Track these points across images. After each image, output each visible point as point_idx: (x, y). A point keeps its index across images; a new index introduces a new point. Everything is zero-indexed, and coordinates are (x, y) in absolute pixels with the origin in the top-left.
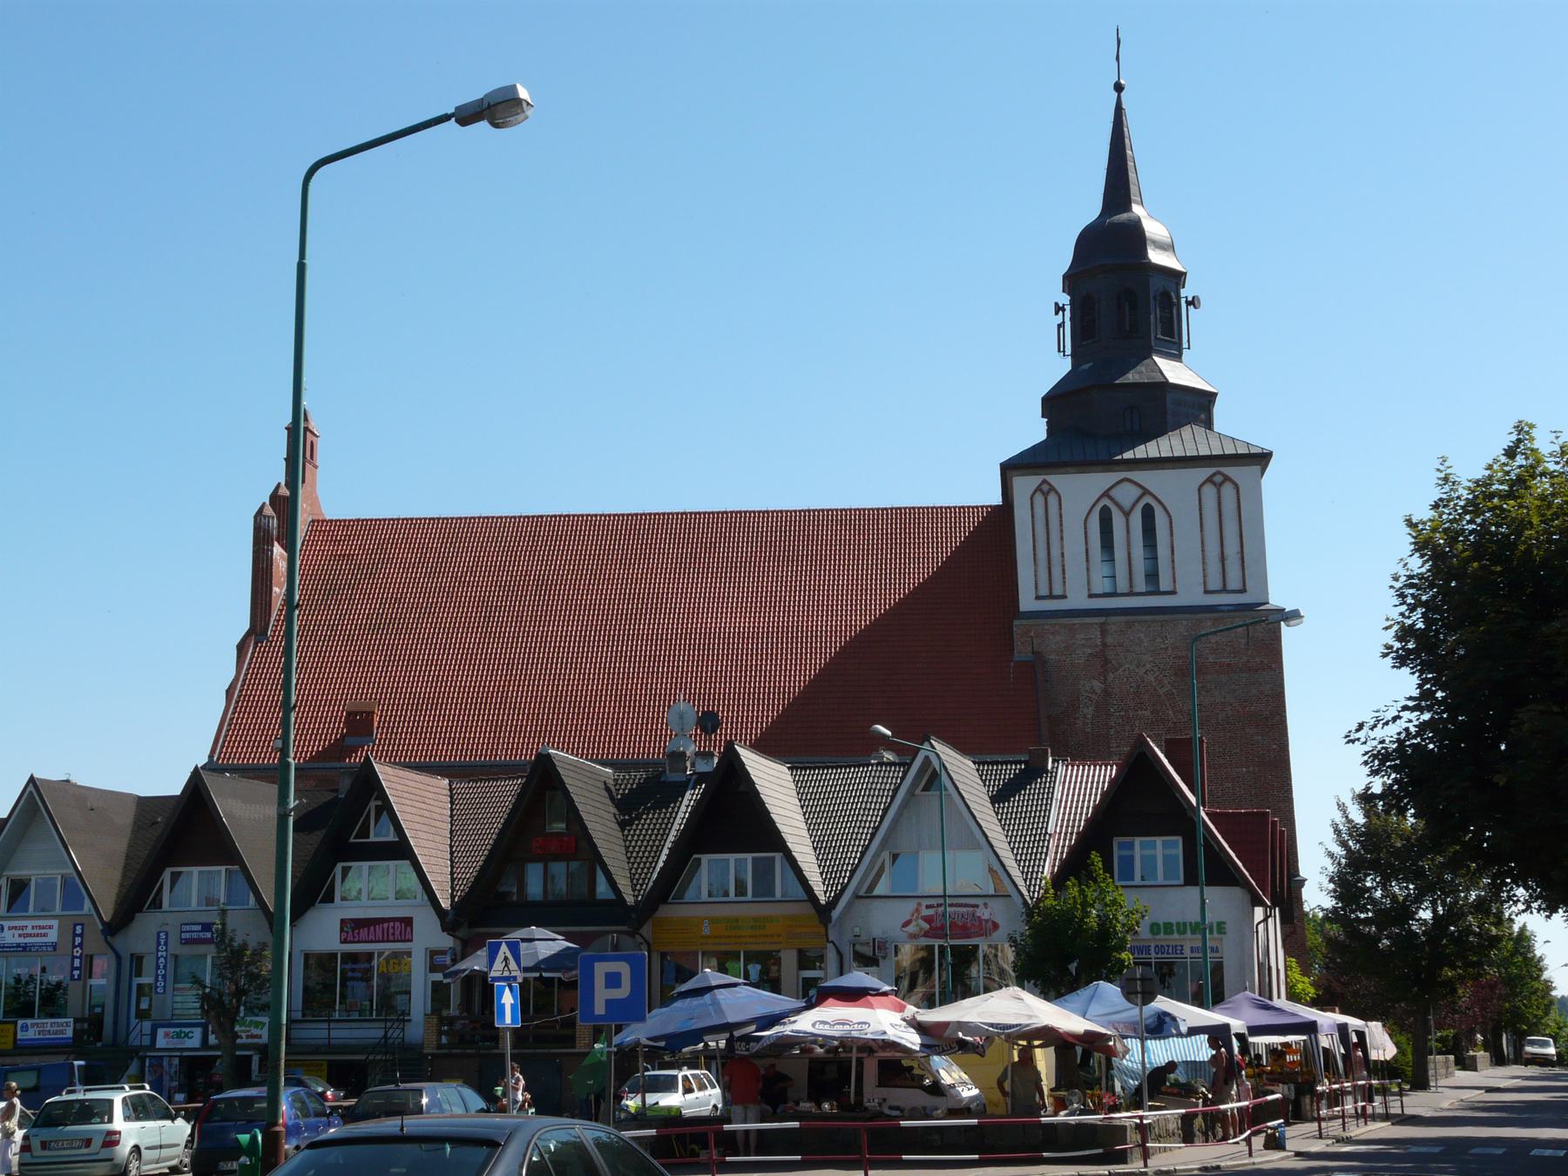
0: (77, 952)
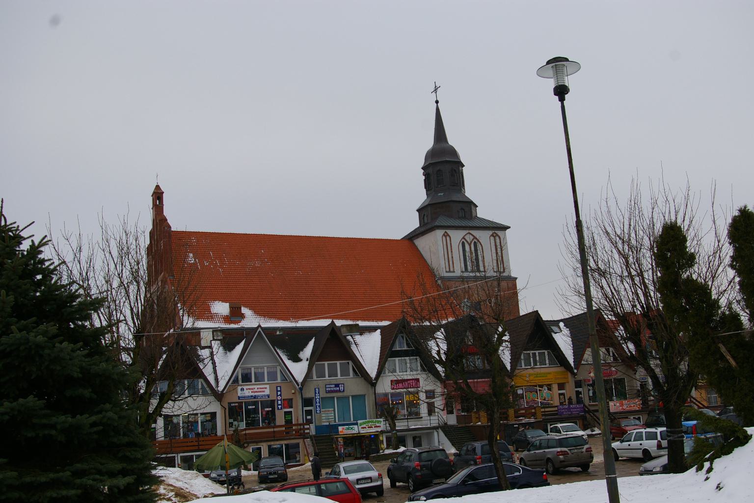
0: (279, 398)
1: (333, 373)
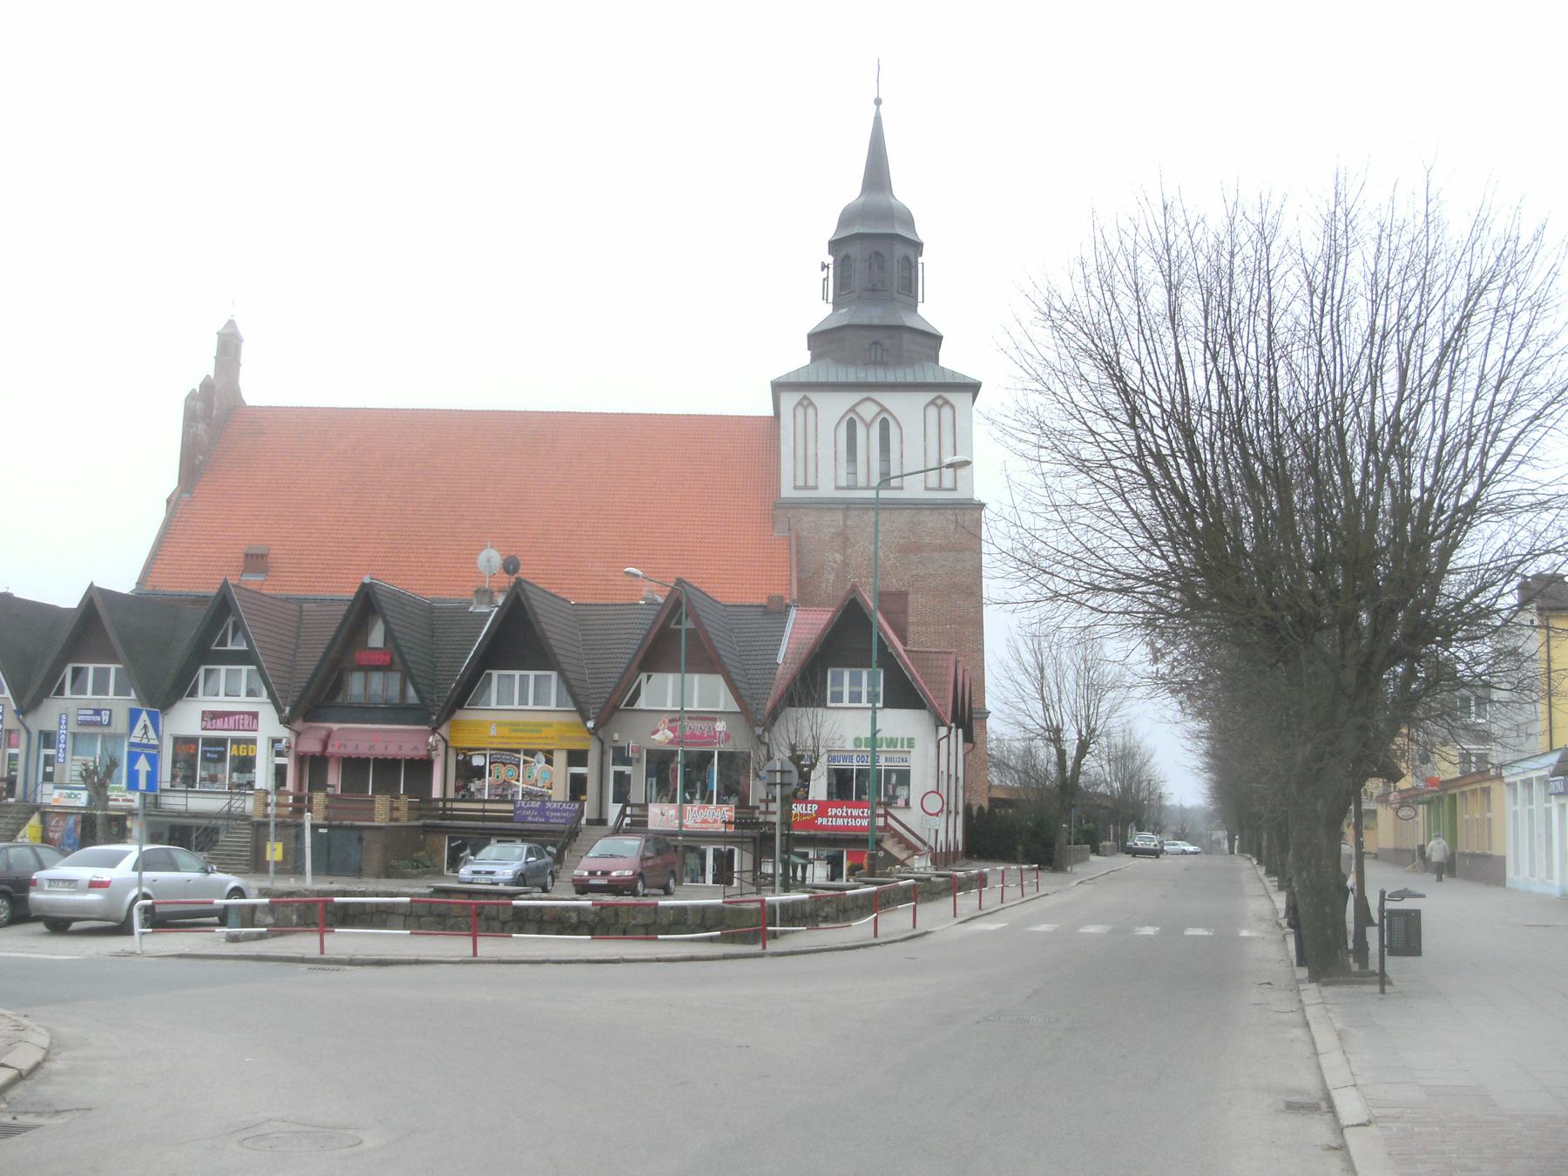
1: (101, 688)
